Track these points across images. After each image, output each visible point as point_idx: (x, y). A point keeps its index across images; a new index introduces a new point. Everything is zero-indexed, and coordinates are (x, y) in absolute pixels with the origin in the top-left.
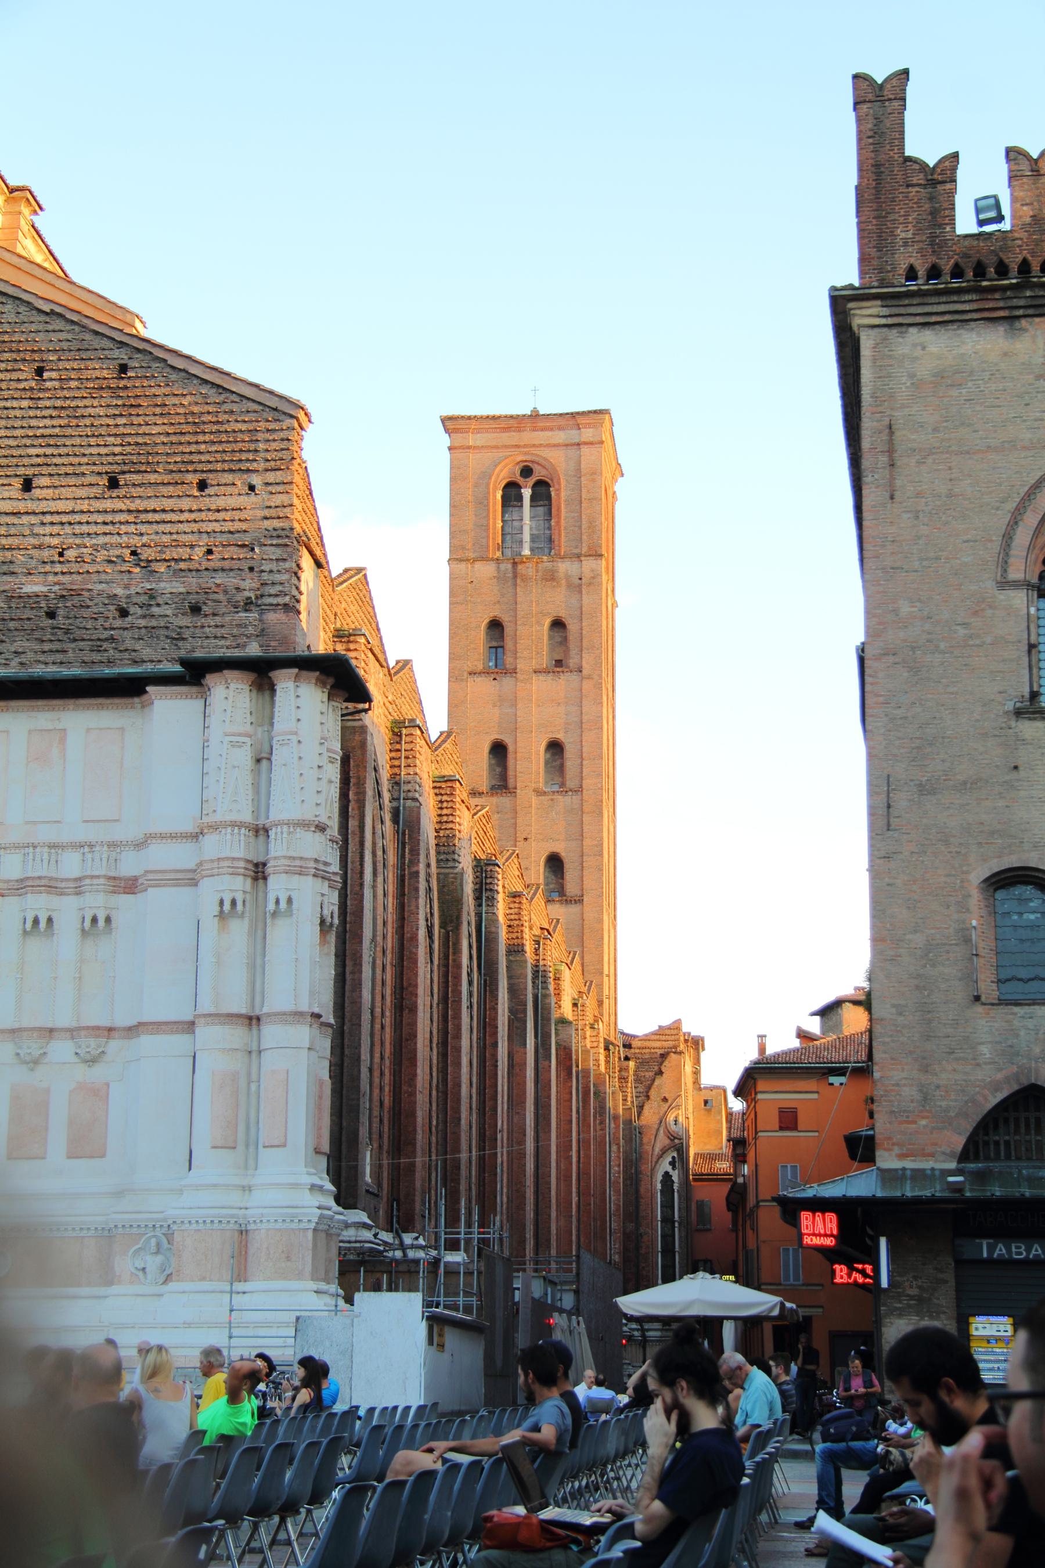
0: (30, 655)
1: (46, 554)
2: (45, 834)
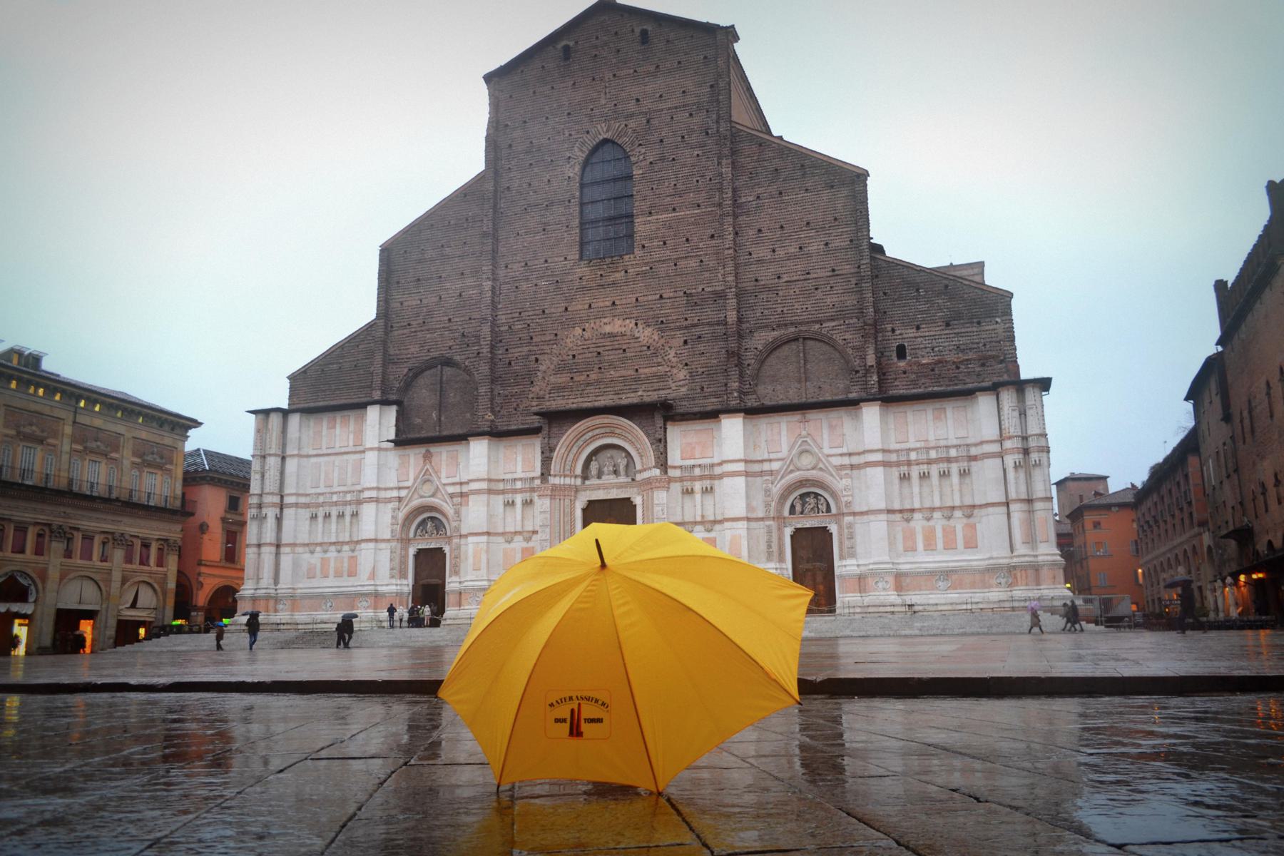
0: (927, 384)
1: (928, 350)
2: (943, 443)
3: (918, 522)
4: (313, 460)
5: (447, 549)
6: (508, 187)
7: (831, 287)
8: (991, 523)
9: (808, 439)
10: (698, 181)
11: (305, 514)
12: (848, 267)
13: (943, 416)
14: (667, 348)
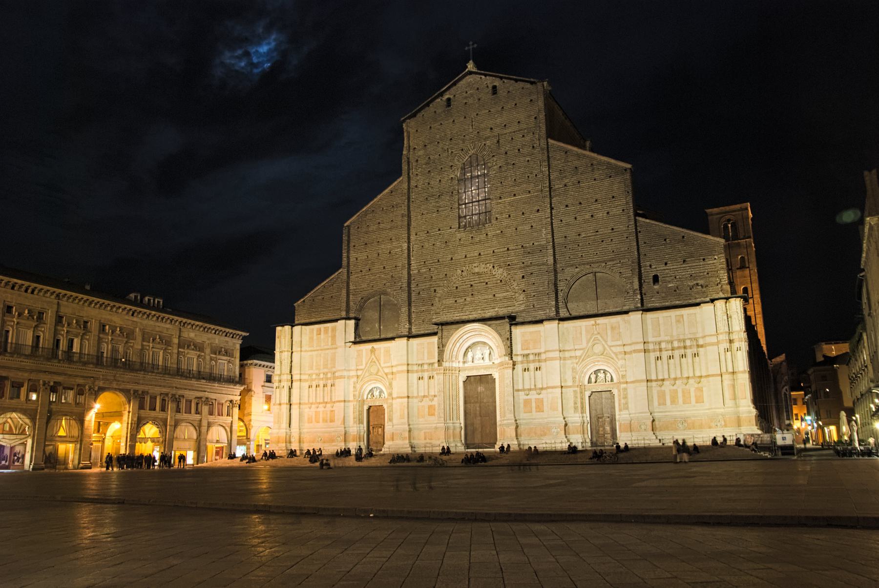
1: (673, 278)
2: (682, 337)
3: (667, 386)
4: (310, 353)
5: (385, 406)
6: (416, 186)
7: (612, 240)
8: (712, 386)
9: (599, 336)
10: (528, 177)
11: (305, 385)
12: (621, 227)
13: (681, 319)
14: (512, 281)
